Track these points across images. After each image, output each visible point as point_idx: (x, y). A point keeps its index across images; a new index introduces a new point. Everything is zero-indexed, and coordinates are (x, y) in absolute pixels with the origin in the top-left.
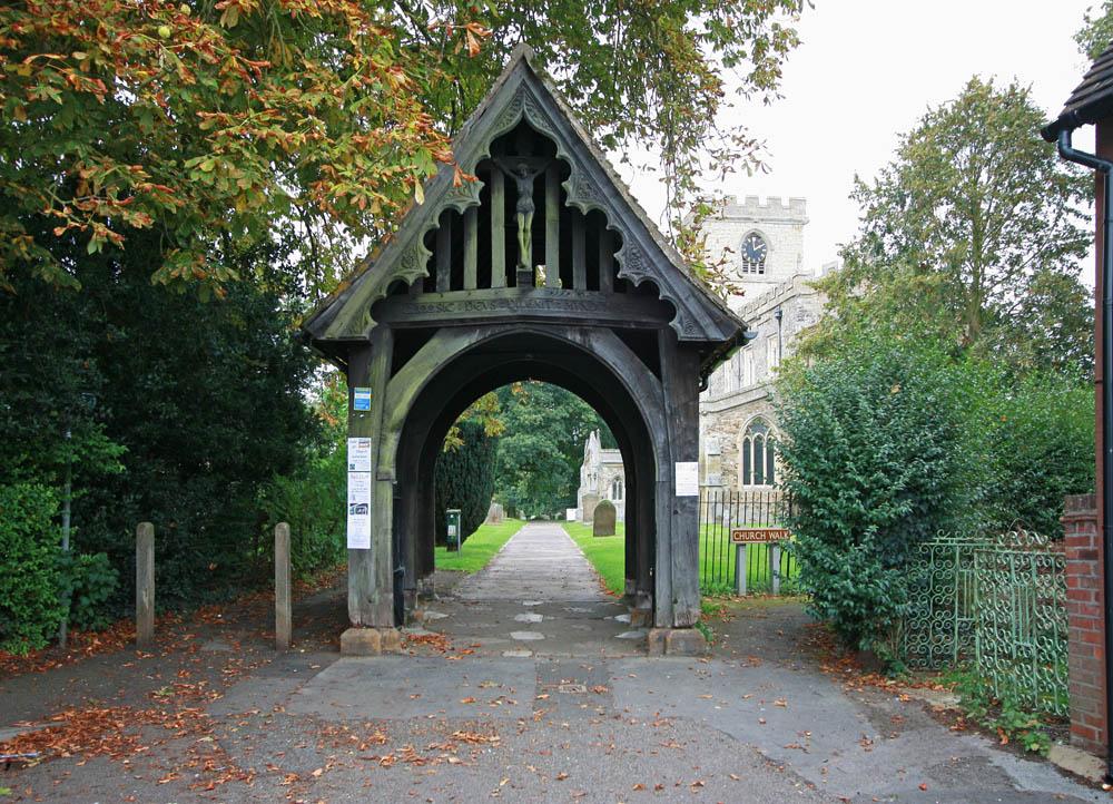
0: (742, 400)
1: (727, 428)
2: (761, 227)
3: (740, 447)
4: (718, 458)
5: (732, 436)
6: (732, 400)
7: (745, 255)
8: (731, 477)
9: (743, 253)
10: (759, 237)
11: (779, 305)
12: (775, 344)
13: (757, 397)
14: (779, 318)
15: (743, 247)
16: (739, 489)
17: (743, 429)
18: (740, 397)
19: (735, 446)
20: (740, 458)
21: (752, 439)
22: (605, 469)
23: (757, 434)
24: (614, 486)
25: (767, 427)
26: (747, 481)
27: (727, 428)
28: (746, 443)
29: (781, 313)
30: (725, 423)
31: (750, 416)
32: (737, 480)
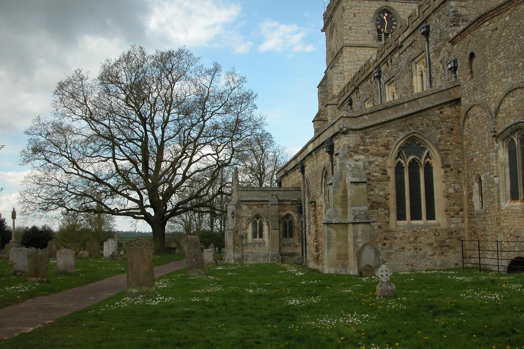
0: (391, 115)
1: (373, 149)
2: (392, 4)
3: (391, 173)
4: (363, 187)
5: (380, 159)
6: (378, 115)
7: (379, 27)
8: (381, 211)
9: (377, 25)
10: (389, 13)
11: (425, 21)
12: (420, 67)
13: (411, 111)
14: (426, 34)
15: (377, 20)
16: (392, 226)
17: (394, 152)
18: (390, 112)
19: (384, 172)
20: (391, 187)
21: (406, 163)
22: (244, 207)
23: (411, 158)
24: (255, 224)
25: (424, 149)
26: (401, 216)
27: (373, 149)
28: (399, 169)
29: (428, 27)
30: (371, 143)
31: (402, 135)
32: (388, 215)
